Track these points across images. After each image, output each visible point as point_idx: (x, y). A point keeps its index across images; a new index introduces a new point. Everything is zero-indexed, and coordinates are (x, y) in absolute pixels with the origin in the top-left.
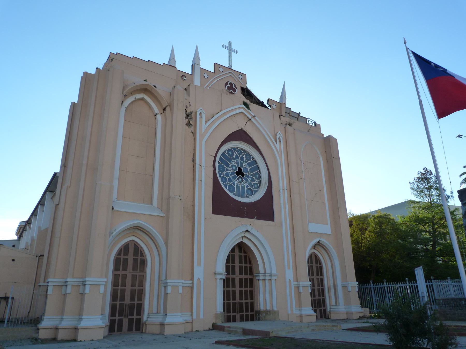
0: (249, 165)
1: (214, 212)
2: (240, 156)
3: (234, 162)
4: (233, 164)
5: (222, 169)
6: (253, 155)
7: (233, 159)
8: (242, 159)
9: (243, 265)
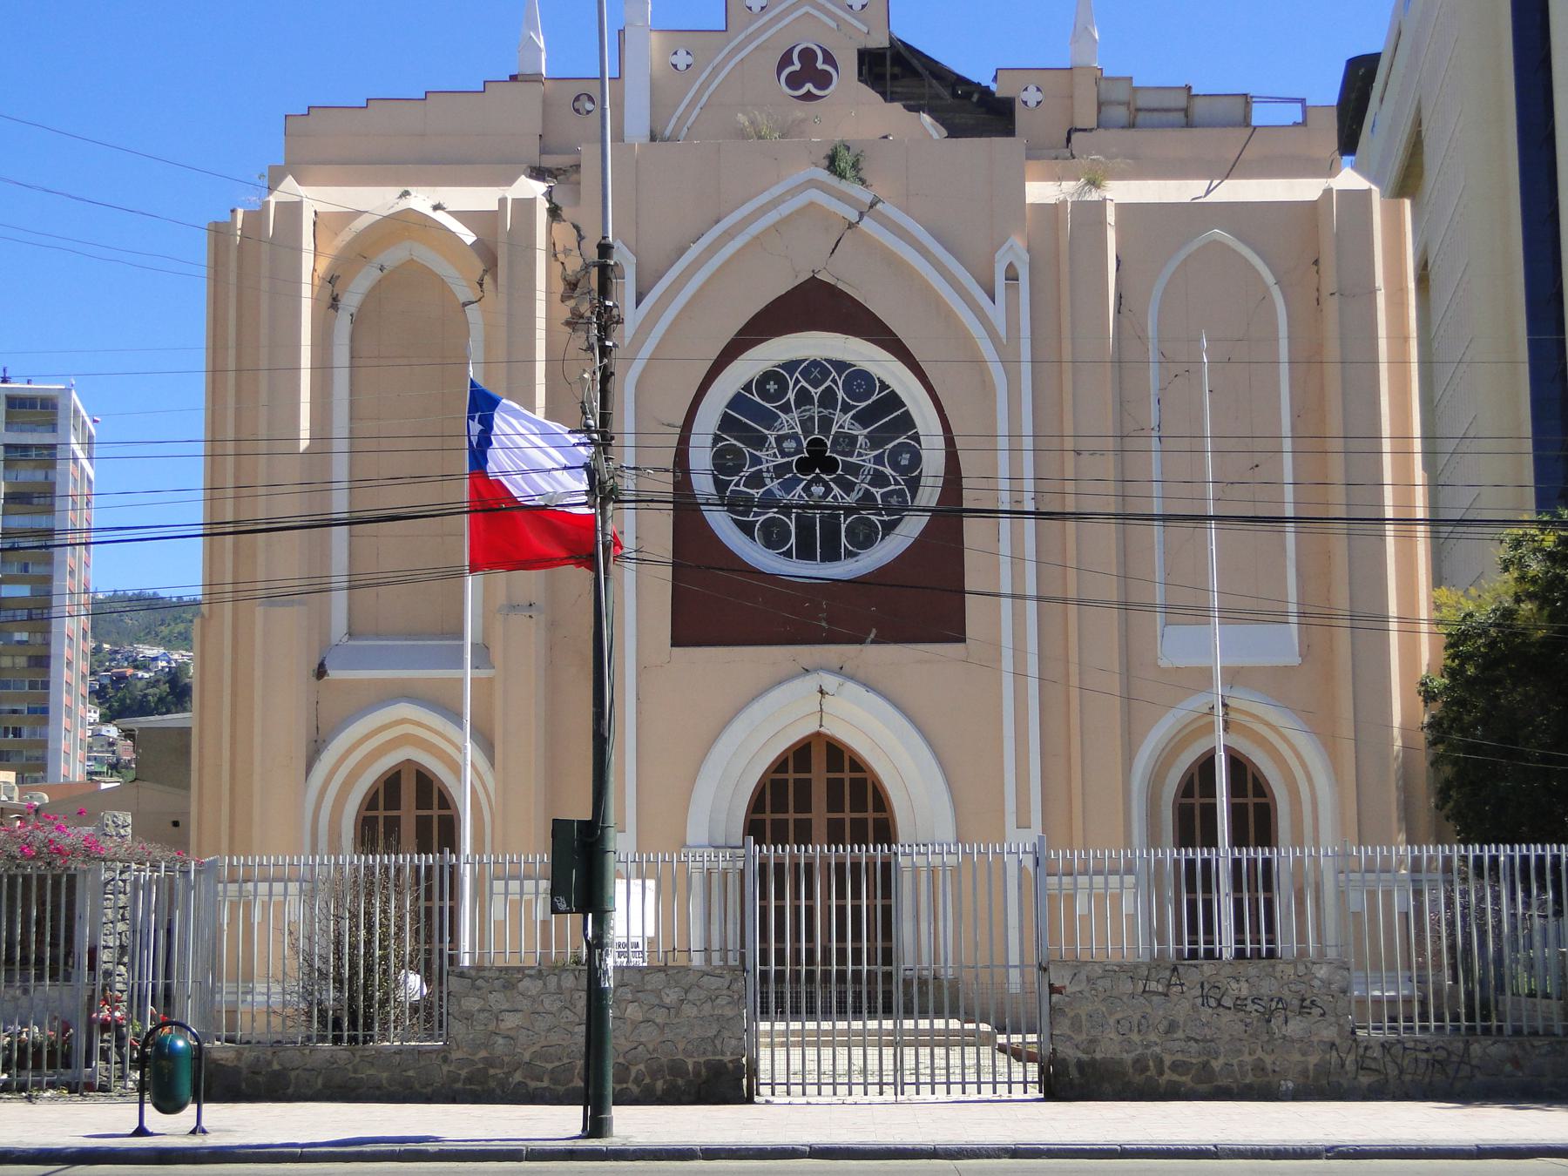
0: (863, 418)
1: (681, 638)
2: (816, 393)
3: (790, 422)
4: (785, 431)
5: (725, 463)
6: (883, 378)
7: (786, 408)
8: (828, 399)
9: (847, 815)
